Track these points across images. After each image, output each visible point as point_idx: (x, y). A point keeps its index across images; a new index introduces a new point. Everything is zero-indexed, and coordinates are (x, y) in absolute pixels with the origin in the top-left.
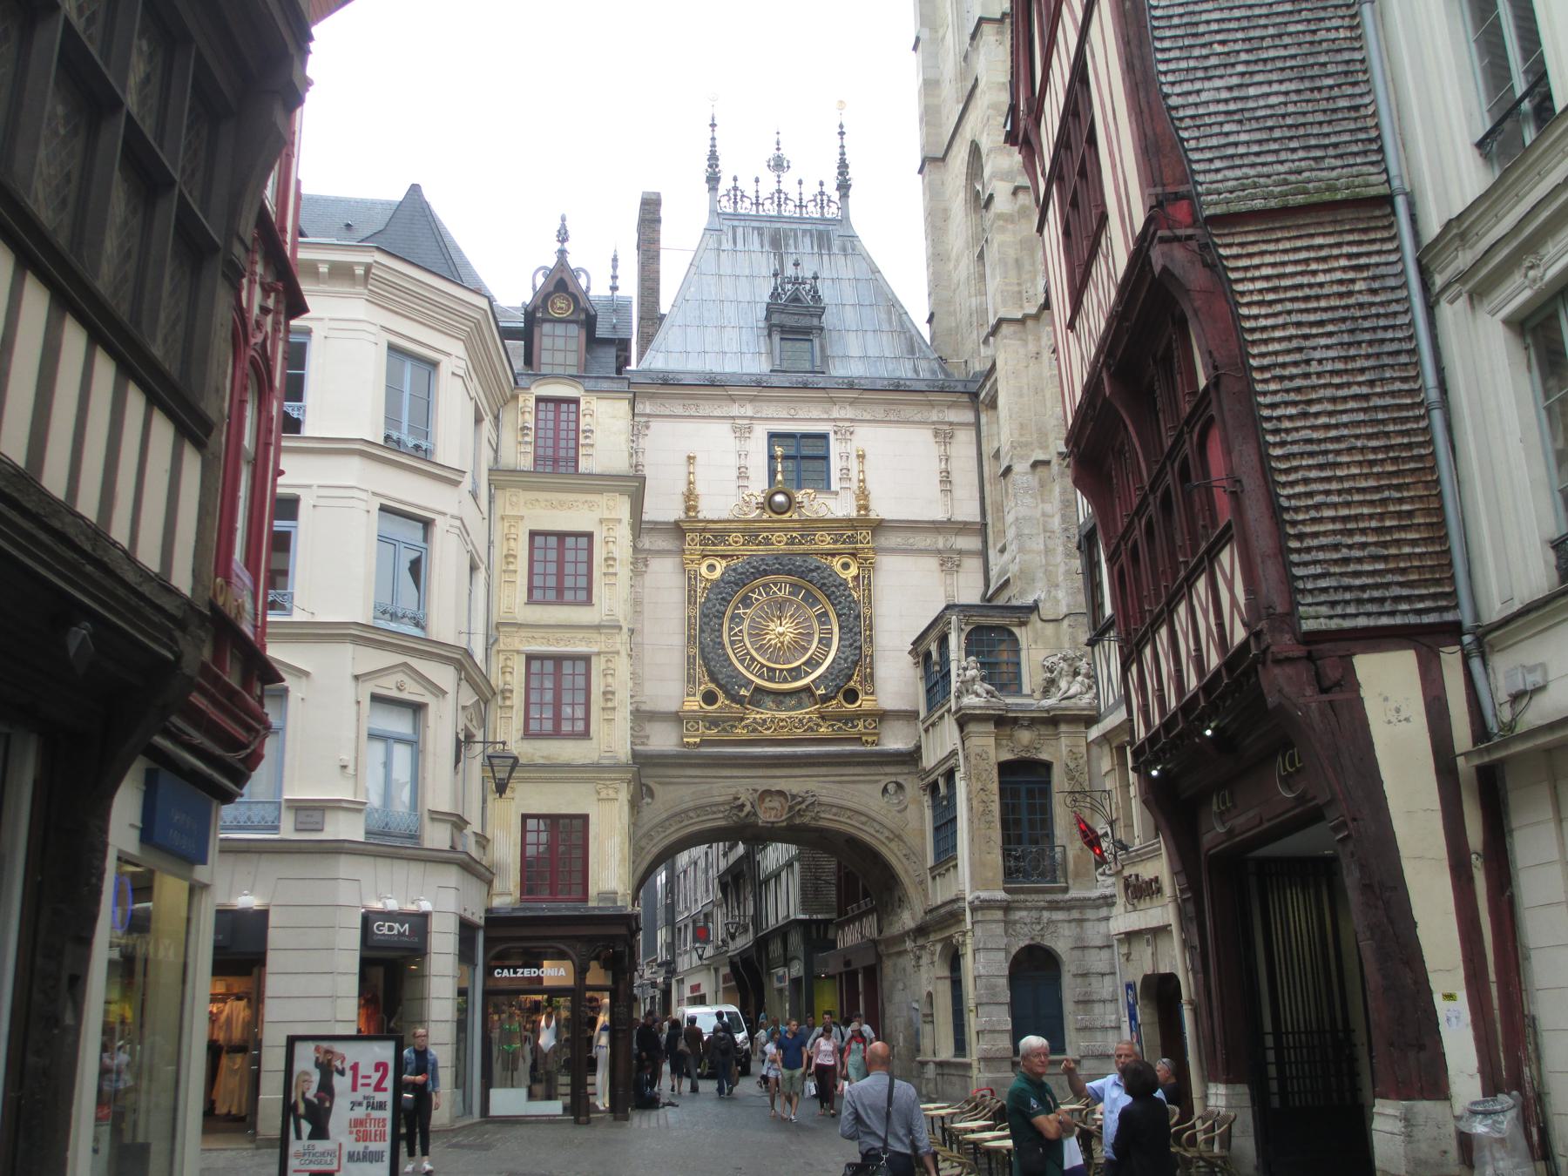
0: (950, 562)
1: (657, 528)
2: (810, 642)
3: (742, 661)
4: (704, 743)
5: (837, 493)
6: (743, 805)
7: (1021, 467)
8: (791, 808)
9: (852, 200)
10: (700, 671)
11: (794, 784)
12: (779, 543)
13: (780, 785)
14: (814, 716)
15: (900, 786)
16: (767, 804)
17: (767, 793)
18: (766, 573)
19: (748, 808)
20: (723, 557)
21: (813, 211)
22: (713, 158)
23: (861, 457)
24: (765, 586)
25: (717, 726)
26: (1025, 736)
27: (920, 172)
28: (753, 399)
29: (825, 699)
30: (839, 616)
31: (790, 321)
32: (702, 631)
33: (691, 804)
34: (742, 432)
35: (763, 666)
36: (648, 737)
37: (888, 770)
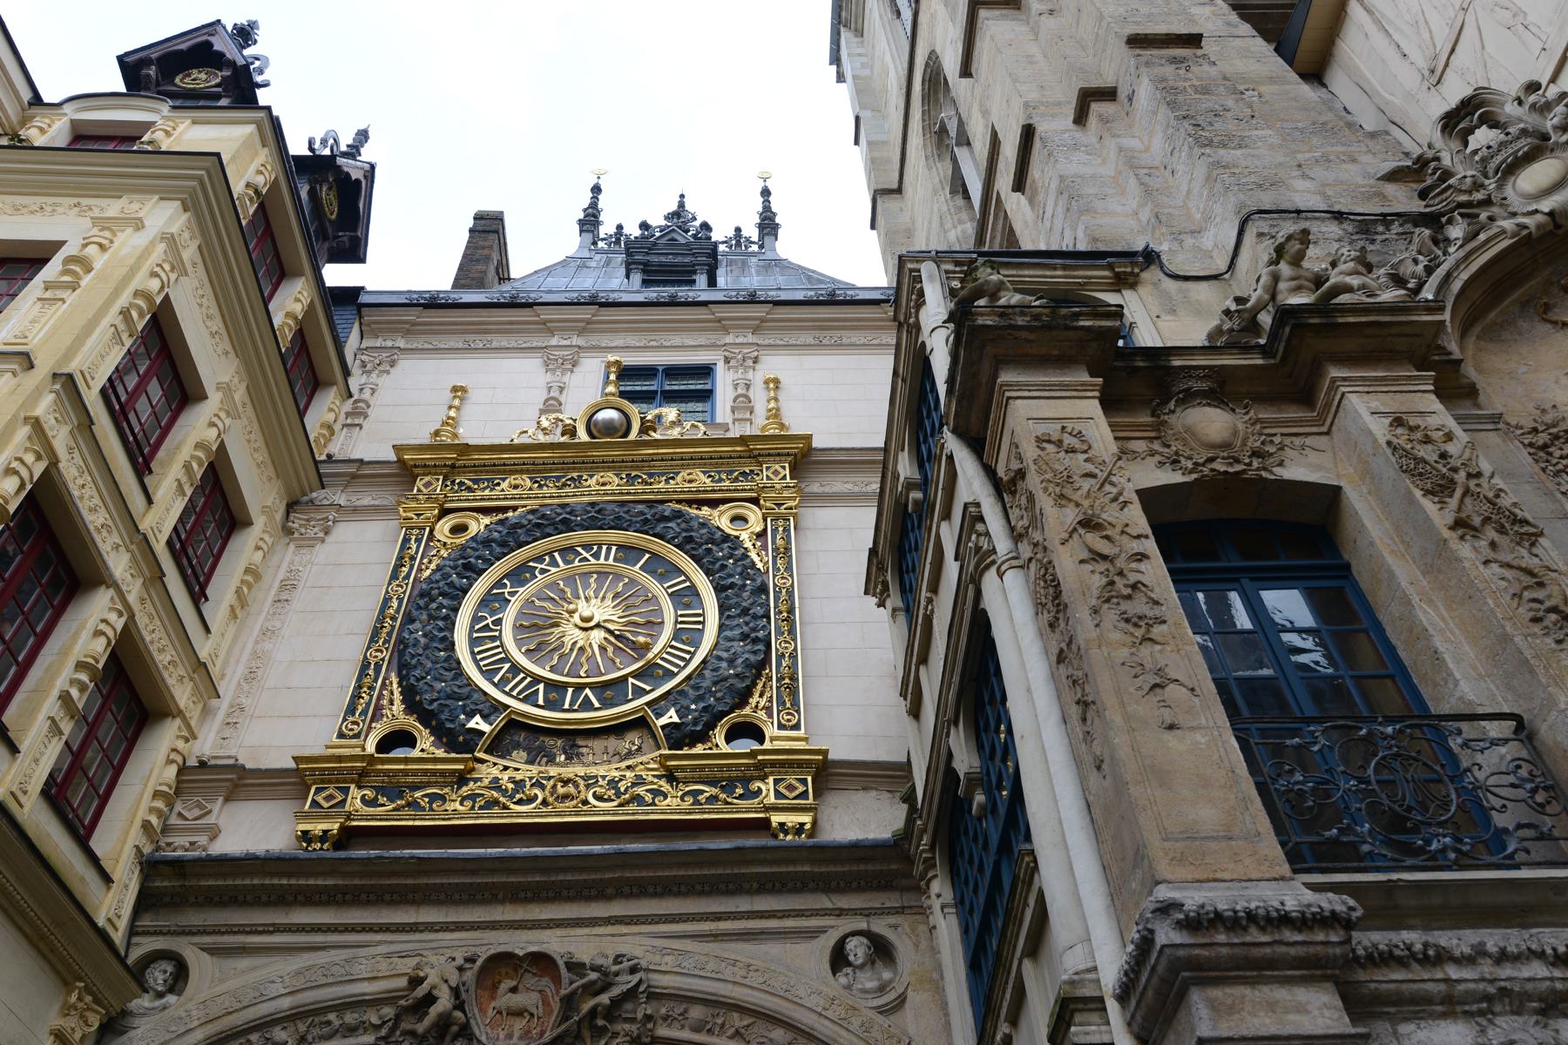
1: (359, 473)
2: (655, 638)
3: (488, 674)
4: (349, 836)
7: (1056, 126)
8: (569, 1002)
11: (584, 940)
12: (602, 485)
13: (554, 943)
15: (882, 950)
16: (506, 1000)
17: (502, 962)
18: (567, 526)
19: (444, 1002)
24: (564, 551)
26: (1212, 421)
27: (873, 227)
28: (585, 328)
29: (679, 737)
30: (719, 589)
31: (655, 259)
32: (409, 619)
33: (286, 1003)
35: (537, 679)
36: (214, 833)
37: (844, 902)
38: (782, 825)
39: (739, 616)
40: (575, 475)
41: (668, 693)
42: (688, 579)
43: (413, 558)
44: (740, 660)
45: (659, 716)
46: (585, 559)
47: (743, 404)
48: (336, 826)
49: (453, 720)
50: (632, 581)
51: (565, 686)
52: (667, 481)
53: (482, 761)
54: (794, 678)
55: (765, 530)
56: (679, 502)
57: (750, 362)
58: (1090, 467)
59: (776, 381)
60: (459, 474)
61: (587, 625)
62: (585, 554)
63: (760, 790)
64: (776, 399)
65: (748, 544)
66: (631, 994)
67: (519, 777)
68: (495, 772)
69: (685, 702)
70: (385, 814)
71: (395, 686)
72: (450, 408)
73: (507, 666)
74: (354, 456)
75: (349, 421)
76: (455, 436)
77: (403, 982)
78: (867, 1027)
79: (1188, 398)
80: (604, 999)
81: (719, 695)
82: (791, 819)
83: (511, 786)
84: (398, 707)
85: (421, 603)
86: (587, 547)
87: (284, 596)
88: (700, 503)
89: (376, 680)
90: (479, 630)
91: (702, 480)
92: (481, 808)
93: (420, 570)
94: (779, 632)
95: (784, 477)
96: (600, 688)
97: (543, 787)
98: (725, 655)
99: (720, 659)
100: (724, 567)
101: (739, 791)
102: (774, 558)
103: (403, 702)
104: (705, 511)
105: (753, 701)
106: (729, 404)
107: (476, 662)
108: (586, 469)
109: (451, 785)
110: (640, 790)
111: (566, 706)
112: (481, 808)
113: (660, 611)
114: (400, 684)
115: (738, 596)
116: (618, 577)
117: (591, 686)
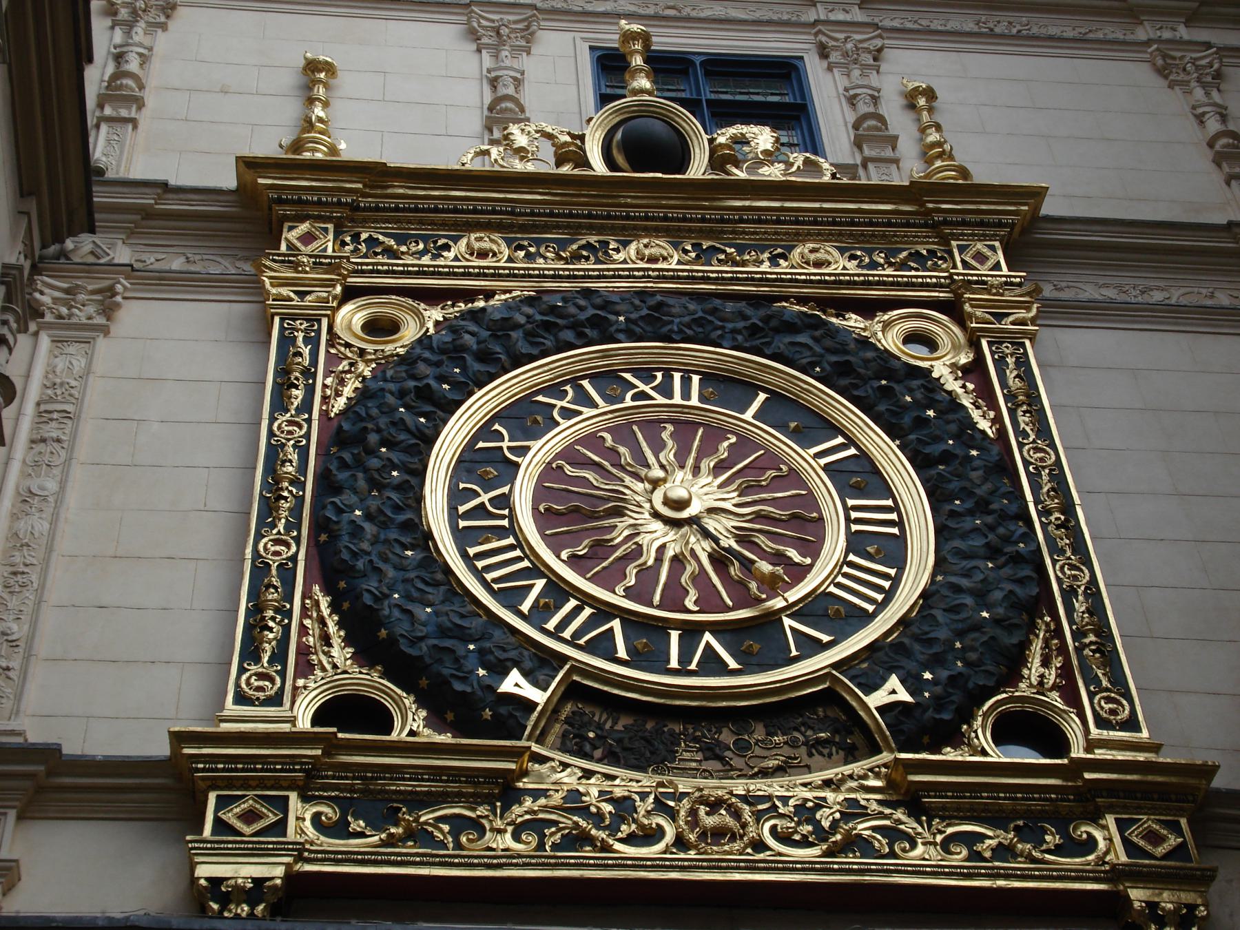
3: (511, 598)
10: (312, 609)
14: (871, 802)
20: (432, 297)
23: (920, 100)
30: (921, 462)
32: (326, 484)
35: (605, 612)
38: (1152, 906)
39: (971, 513)
40: (593, 239)
41: (872, 647)
42: (851, 442)
43: (309, 373)
44: (997, 595)
45: (870, 689)
46: (642, 395)
47: (870, 131)
48: (279, 871)
50: (745, 444)
51: (660, 628)
52: (774, 260)
53: (542, 760)
55: (979, 359)
56: (802, 300)
57: (867, 59)
59: (930, 94)
60: (364, 222)
61: (675, 516)
62: (642, 387)
63: (1091, 843)
64: (938, 128)
65: (953, 385)
67: (619, 792)
68: (569, 779)
69: (911, 665)
70: (363, 852)
71: (326, 612)
72: (311, 101)
73: (540, 584)
74: (137, 173)
75: (108, 111)
76: (333, 150)
81: (973, 656)
83: (607, 808)
84: (340, 653)
86: (647, 375)
87: (51, 431)
88: (844, 306)
89: (289, 598)
90: (467, 515)
91: (841, 265)
92: (555, 847)
93: (325, 399)
95: (997, 266)
97: (672, 815)
98: (965, 582)
99: (957, 589)
100: (923, 422)
101: (1051, 839)
102: (1012, 413)
103: (348, 641)
104: (854, 321)
105: (1034, 669)
107: (479, 574)
108: (613, 230)
109: (489, 800)
110: (863, 828)
111: (674, 663)
113: (810, 500)
114: (335, 607)
116: (715, 434)
117: (717, 629)
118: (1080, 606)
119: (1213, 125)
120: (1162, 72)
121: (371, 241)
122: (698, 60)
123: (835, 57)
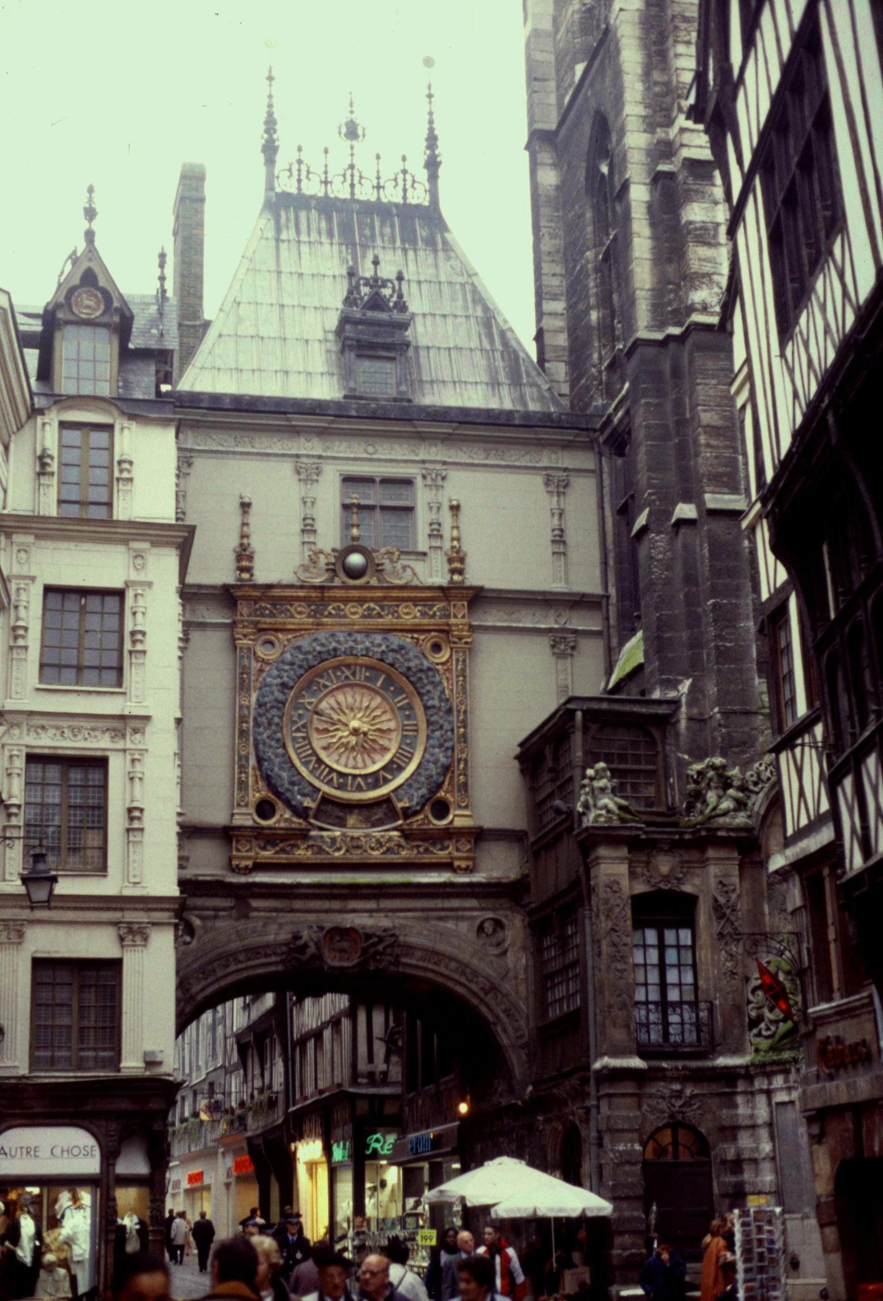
0: (563, 644)
3: (306, 764)
5: (425, 554)
6: (305, 946)
9: (441, 182)
19: (312, 949)
21: (392, 195)
22: (270, 124)
23: (455, 509)
25: (274, 845)
26: (664, 864)
32: (257, 725)
34: (308, 474)
38: (459, 867)
45: (400, 800)
49: (295, 799)
54: (465, 775)
57: (440, 482)
58: (619, 901)
64: (458, 528)
66: (392, 945)
70: (267, 854)
77: (290, 936)
78: (491, 962)
79: (661, 850)
80: (380, 948)
82: (463, 864)
85: (261, 711)
94: (459, 742)
96: (365, 777)
99: (428, 762)
106: (427, 531)
112: (317, 853)
115: (436, 714)
117: (360, 776)
118: (462, 766)
119: (556, 521)
120: (547, 484)
121: (266, 608)
122: (378, 480)
123: (429, 482)
